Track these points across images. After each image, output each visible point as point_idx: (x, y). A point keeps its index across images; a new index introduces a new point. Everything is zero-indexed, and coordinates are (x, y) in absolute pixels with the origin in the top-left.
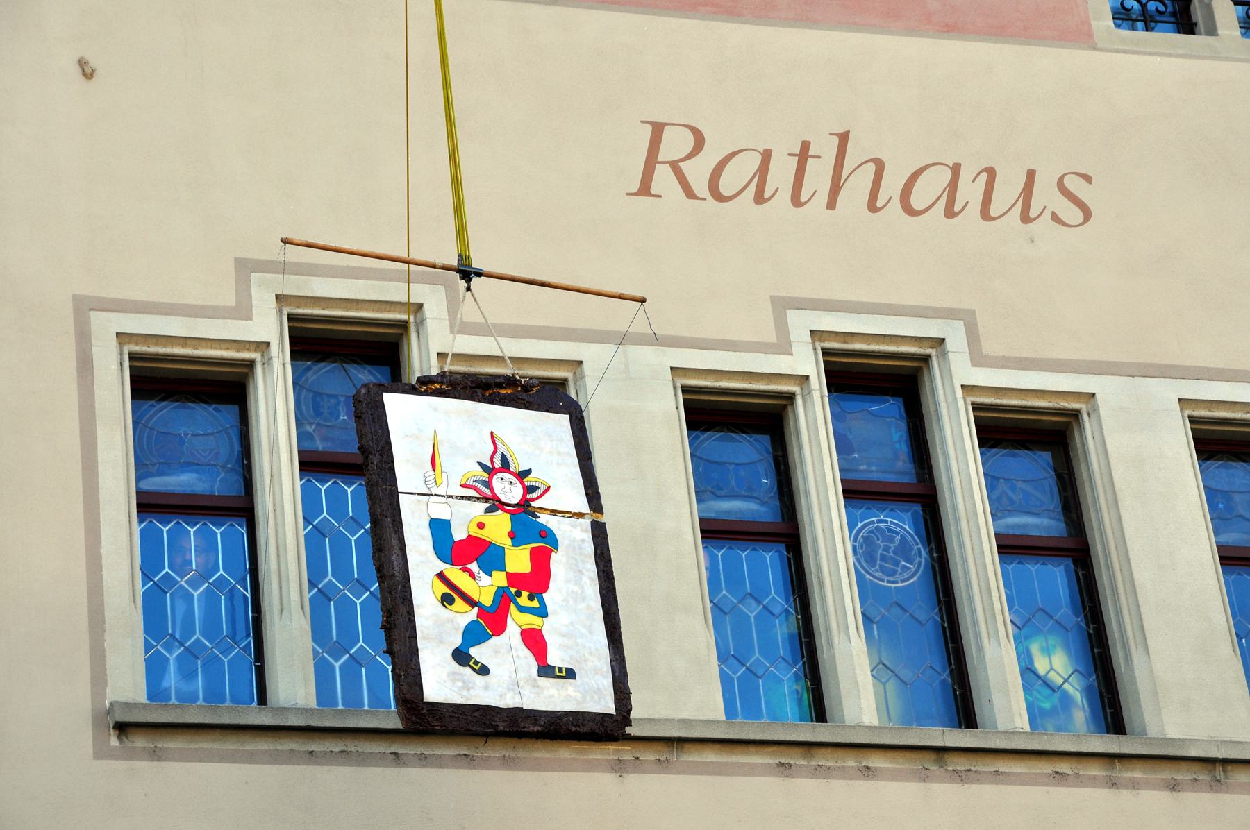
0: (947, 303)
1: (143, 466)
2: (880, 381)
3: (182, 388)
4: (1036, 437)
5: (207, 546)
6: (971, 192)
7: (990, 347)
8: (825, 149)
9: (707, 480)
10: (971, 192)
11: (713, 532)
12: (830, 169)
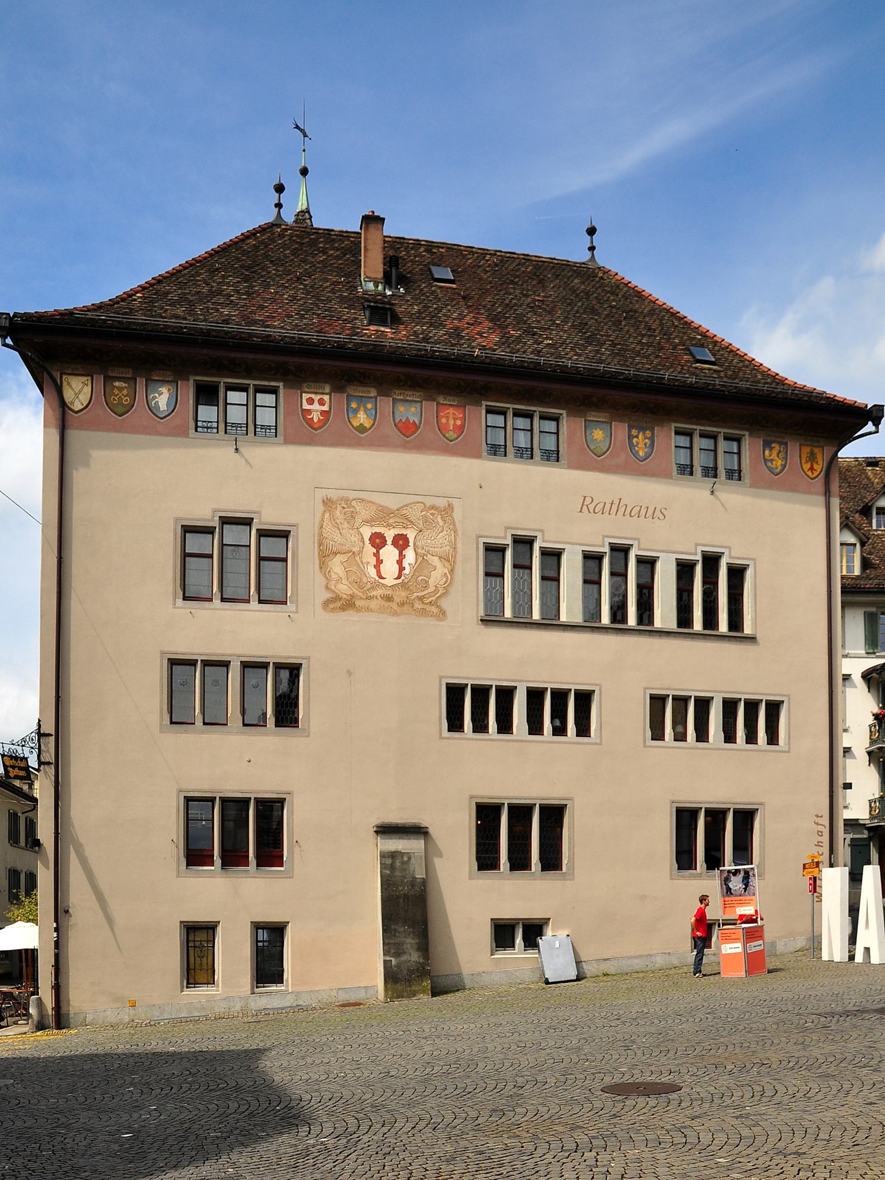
0: (635, 536)
1: (486, 565)
2: (620, 551)
3: (494, 551)
4: (648, 564)
5: (496, 583)
6: (643, 512)
7: (641, 546)
8: (616, 502)
9: (585, 571)
10: (643, 512)
11: (585, 582)
12: (616, 507)
